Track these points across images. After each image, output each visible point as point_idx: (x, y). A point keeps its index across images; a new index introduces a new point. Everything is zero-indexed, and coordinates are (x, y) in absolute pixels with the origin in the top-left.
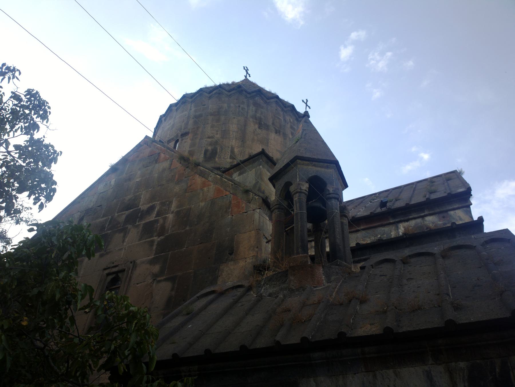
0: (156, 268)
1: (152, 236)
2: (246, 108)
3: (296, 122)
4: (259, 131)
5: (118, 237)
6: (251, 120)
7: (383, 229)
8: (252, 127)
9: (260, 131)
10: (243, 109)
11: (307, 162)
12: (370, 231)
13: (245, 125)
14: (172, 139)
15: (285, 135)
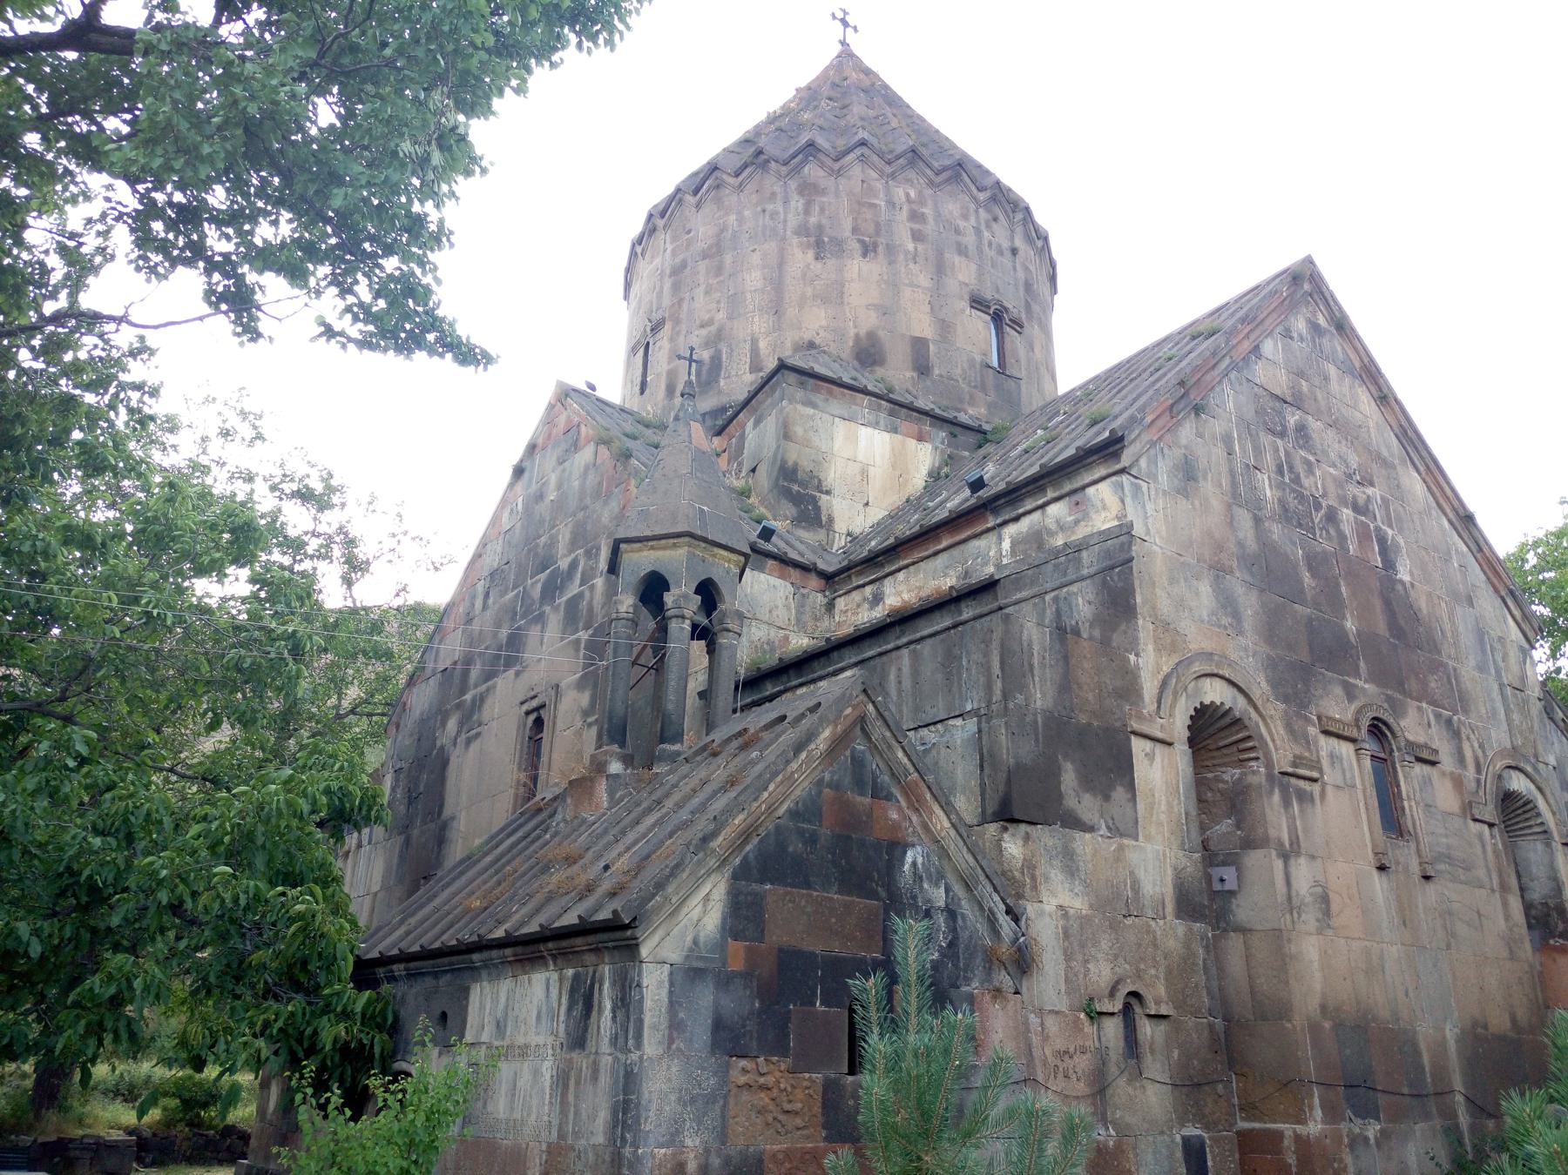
0: (585, 699)
1: (577, 631)
2: (781, 210)
3: (928, 192)
4: (817, 267)
5: (534, 632)
6: (795, 241)
7: (975, 543)
8: (800, 258)
9: (819, 265)
10: (773, 215)
11: (638, 545)
12: (955, 552)
13: (781, 265)
14: (638, 342)
15: (891, 250)
